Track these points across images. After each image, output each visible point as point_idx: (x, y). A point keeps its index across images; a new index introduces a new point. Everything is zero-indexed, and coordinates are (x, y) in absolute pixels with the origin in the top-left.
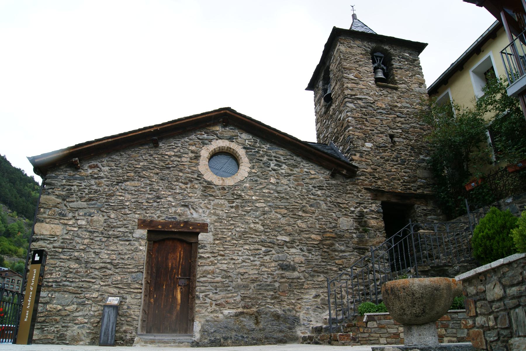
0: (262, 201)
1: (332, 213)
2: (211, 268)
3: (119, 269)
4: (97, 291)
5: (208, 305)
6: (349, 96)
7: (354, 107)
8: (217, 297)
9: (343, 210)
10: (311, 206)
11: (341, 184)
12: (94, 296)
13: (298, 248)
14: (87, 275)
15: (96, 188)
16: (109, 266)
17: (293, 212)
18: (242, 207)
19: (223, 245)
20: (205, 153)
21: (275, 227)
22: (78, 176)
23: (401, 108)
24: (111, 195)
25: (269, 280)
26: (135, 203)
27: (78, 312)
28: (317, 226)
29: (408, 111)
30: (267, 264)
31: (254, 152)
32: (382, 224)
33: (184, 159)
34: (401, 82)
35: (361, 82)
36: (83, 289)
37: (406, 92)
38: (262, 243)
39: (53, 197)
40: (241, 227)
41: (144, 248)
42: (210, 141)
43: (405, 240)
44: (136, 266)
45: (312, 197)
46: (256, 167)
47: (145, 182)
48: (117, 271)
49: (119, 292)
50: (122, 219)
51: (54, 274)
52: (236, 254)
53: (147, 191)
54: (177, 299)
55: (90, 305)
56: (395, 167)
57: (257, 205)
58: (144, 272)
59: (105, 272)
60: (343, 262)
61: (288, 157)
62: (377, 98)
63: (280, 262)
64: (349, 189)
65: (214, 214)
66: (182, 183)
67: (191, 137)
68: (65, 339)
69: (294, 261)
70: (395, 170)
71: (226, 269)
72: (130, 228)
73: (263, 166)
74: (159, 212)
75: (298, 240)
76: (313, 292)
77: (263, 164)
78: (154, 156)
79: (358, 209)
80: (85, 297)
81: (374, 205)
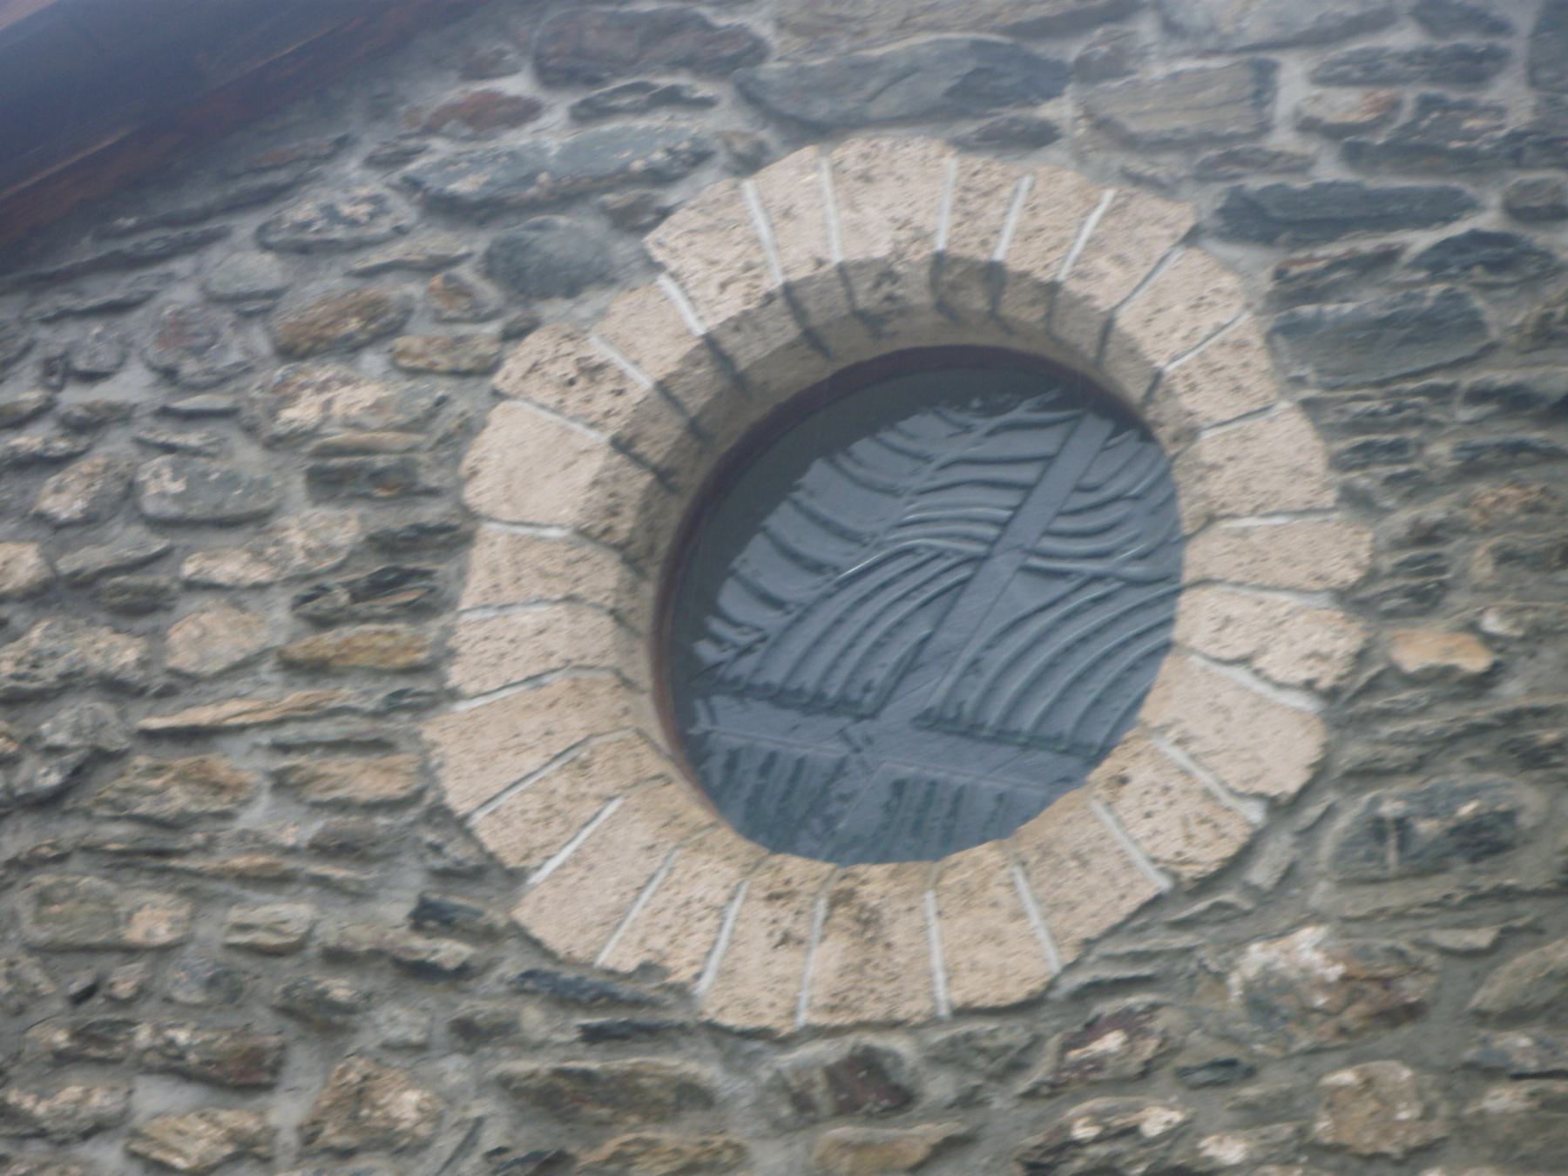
20: (541, 465)
31: (1436, 262)
33: (202, 637)
42: (638, 205)
46: (1482, 567)
66: (174, 1067)
67: (303, 210)
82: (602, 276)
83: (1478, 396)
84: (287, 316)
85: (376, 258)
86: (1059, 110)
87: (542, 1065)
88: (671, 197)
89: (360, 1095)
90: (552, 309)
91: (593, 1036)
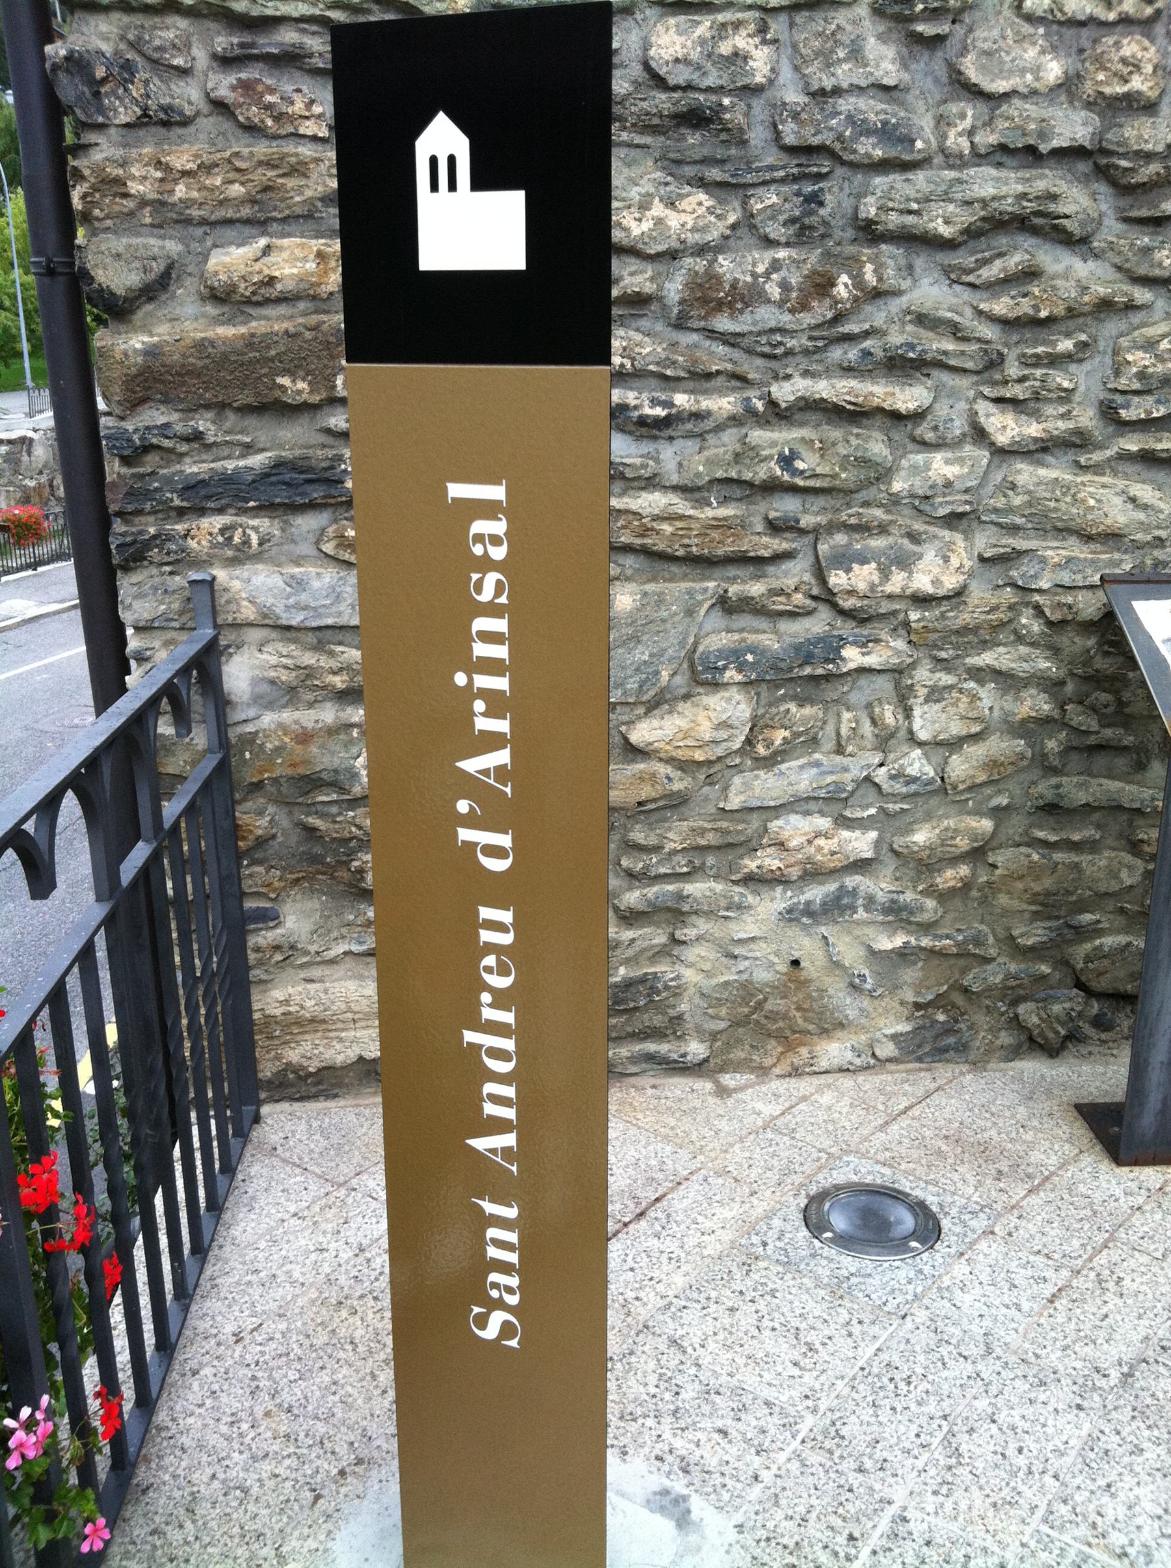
4: (953, 520)
12: (922, 582)
14: (832, 332)
16: (1077, 199)
27: (769, 762)
36: (787, 506)
59: (1031, 274)
68: (674, 1028)
80: (827, 597)
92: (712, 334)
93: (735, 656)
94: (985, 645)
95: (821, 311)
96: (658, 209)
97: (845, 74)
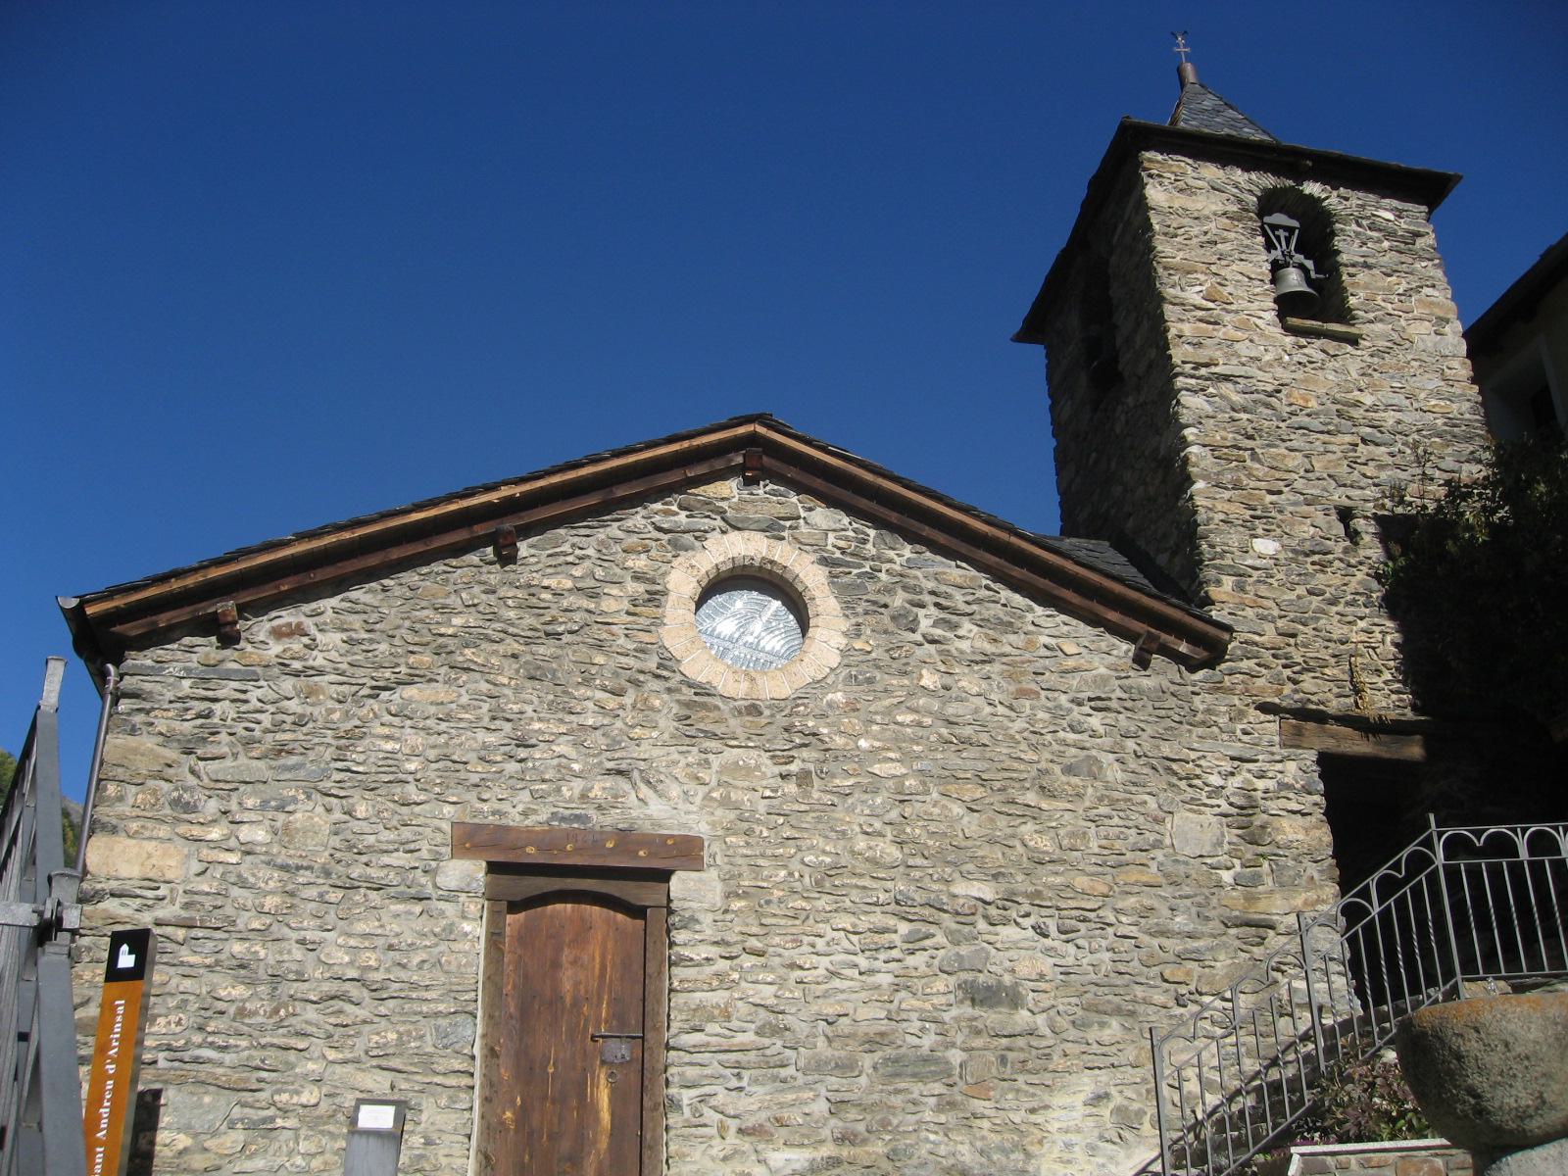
0: (892, 755)
1: (1147, 797)
2: (719, 997)
3: (391, 1003)
5: (713, 1131)
6: (1188, 368)
7: (1209, 409)
8: (743, 1103)
9: (1183, 784)
10: (1069, 770)
11: (1173, 688)
13: (1027, 922)
15: (299, 710)
16: (354, 991)
17: (1003, 790)
18: (822, 775)
19: (759, 915)
20: (682, 580)
21: (941, 851)
22: (235, 666)
23: (1374, 408)
24: (354, 736)
25: (928, 1041)
26: (440, 765)
27: (250, 1157)
28: (1094, 846)
29: (1399, 422)
30: (920, 983)
31: (859, 576)
32: (1325, 835)
33: (607, 605)
34: (1371, 316)
35: (1228, 318)
36: (264, 1074)
37: (1388, 351)
38: (901, 906)
39: (148, 742)
40: (820, 851)
41: (476, 929)
42: (701, 535)
43: (1417, 892)
44: (452, 993)
45: (1071, 737)
47: (473, 686)
48: (383, 1010)
49: (392, 1087)
50: (395, 823)
51: (161, 1021)
52: (805, 949)
53: (479, 719)
54: (596, 1112)
55: (290, 1133)
56: (1362, 624)
57: (876, 769)
58: (479, 1014)
59: (341, 1012)
60: (1188, 973)
61: (983, 593)
62: (1285, 376)
63: (964, 976)
64: (1201, 707)
65: (726, 803)
66: (604, 689)
69: (1013, 971)
70: (1364, 637)
71: (771, 1001)
72: (424, 853)
73: (891, 627)
74: (525, 796)
75: (1027, 895)
76: (1087, 1084)
77: (893, 618)
78: (502, 592)
79: (1235, 782)
80: (274, 1104)
81: (1291, 767)
82: (692, 548)
83: (868, 601)
84: (624, 545)
85: (644, 536)
86: (785, 534)
87: (687, 698)
88: (708, 535)
89: (646, 699)
90: (682, 553)
91: (696, 694)
92: (243, 1023)
93: (242, 1120)
94: (325, 1124)
95: (276, 1019)
96: (229, 989)
97: (286, 957)
